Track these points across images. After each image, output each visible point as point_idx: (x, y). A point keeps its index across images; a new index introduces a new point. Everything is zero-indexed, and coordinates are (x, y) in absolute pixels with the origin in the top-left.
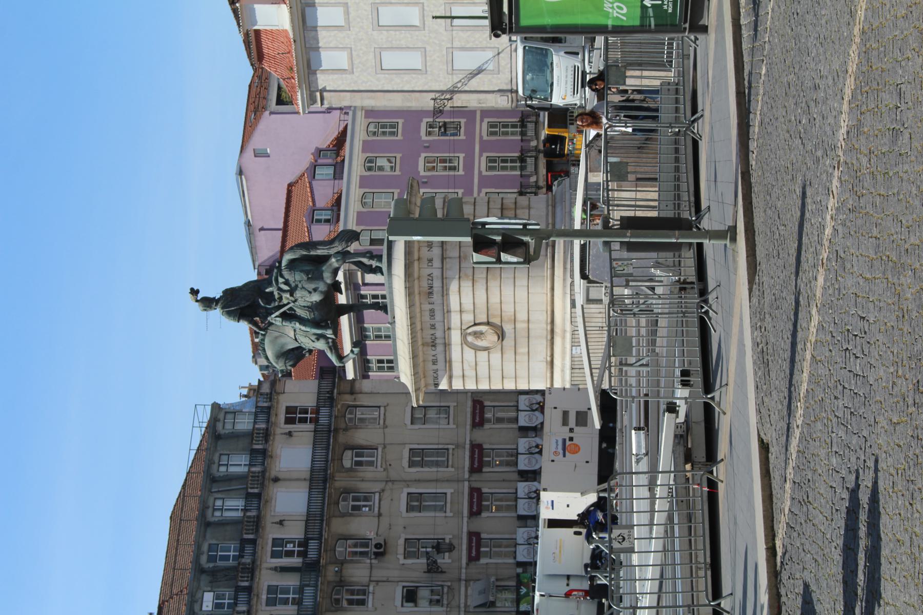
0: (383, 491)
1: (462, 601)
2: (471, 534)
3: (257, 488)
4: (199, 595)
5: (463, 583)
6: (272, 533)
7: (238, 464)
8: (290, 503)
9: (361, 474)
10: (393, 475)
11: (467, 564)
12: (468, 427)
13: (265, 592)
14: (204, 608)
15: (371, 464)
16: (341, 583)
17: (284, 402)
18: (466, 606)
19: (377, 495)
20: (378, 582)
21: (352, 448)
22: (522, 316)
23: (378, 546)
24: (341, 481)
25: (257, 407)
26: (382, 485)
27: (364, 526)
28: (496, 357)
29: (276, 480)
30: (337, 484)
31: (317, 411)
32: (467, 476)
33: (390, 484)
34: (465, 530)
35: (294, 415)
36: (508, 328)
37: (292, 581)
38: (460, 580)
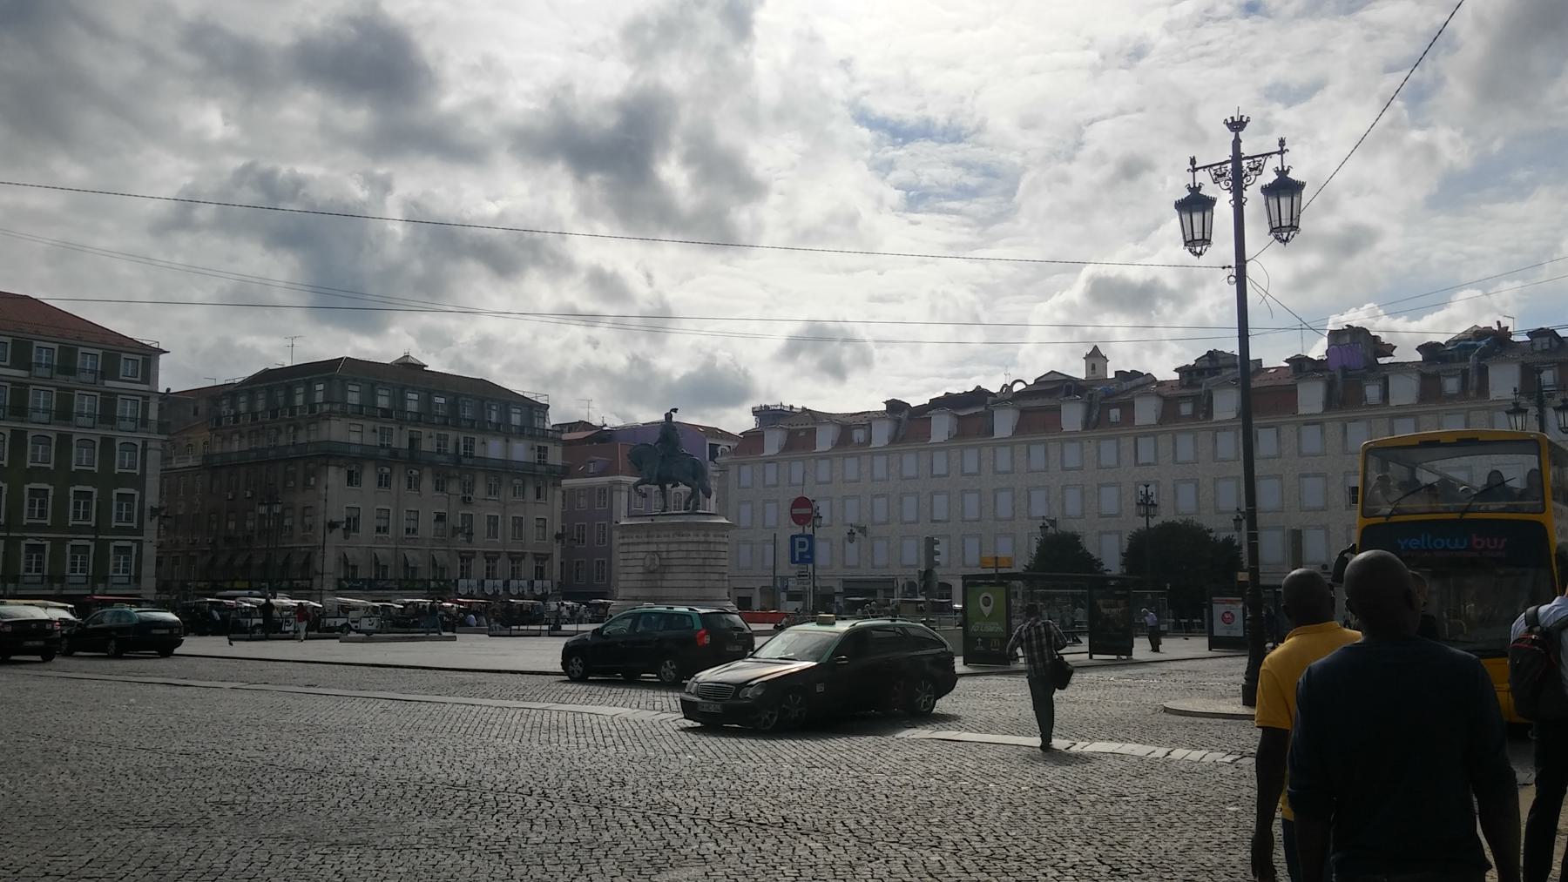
3: (504, 431)
6: (478, 439)
7: (516, 419)
8: (494, 449)
22: (665, 584)
27: (480, 490)
28: (641, 570)
31: (545, 464)
35: (542, 451)
36: (658, 576)
37: (451, 449)
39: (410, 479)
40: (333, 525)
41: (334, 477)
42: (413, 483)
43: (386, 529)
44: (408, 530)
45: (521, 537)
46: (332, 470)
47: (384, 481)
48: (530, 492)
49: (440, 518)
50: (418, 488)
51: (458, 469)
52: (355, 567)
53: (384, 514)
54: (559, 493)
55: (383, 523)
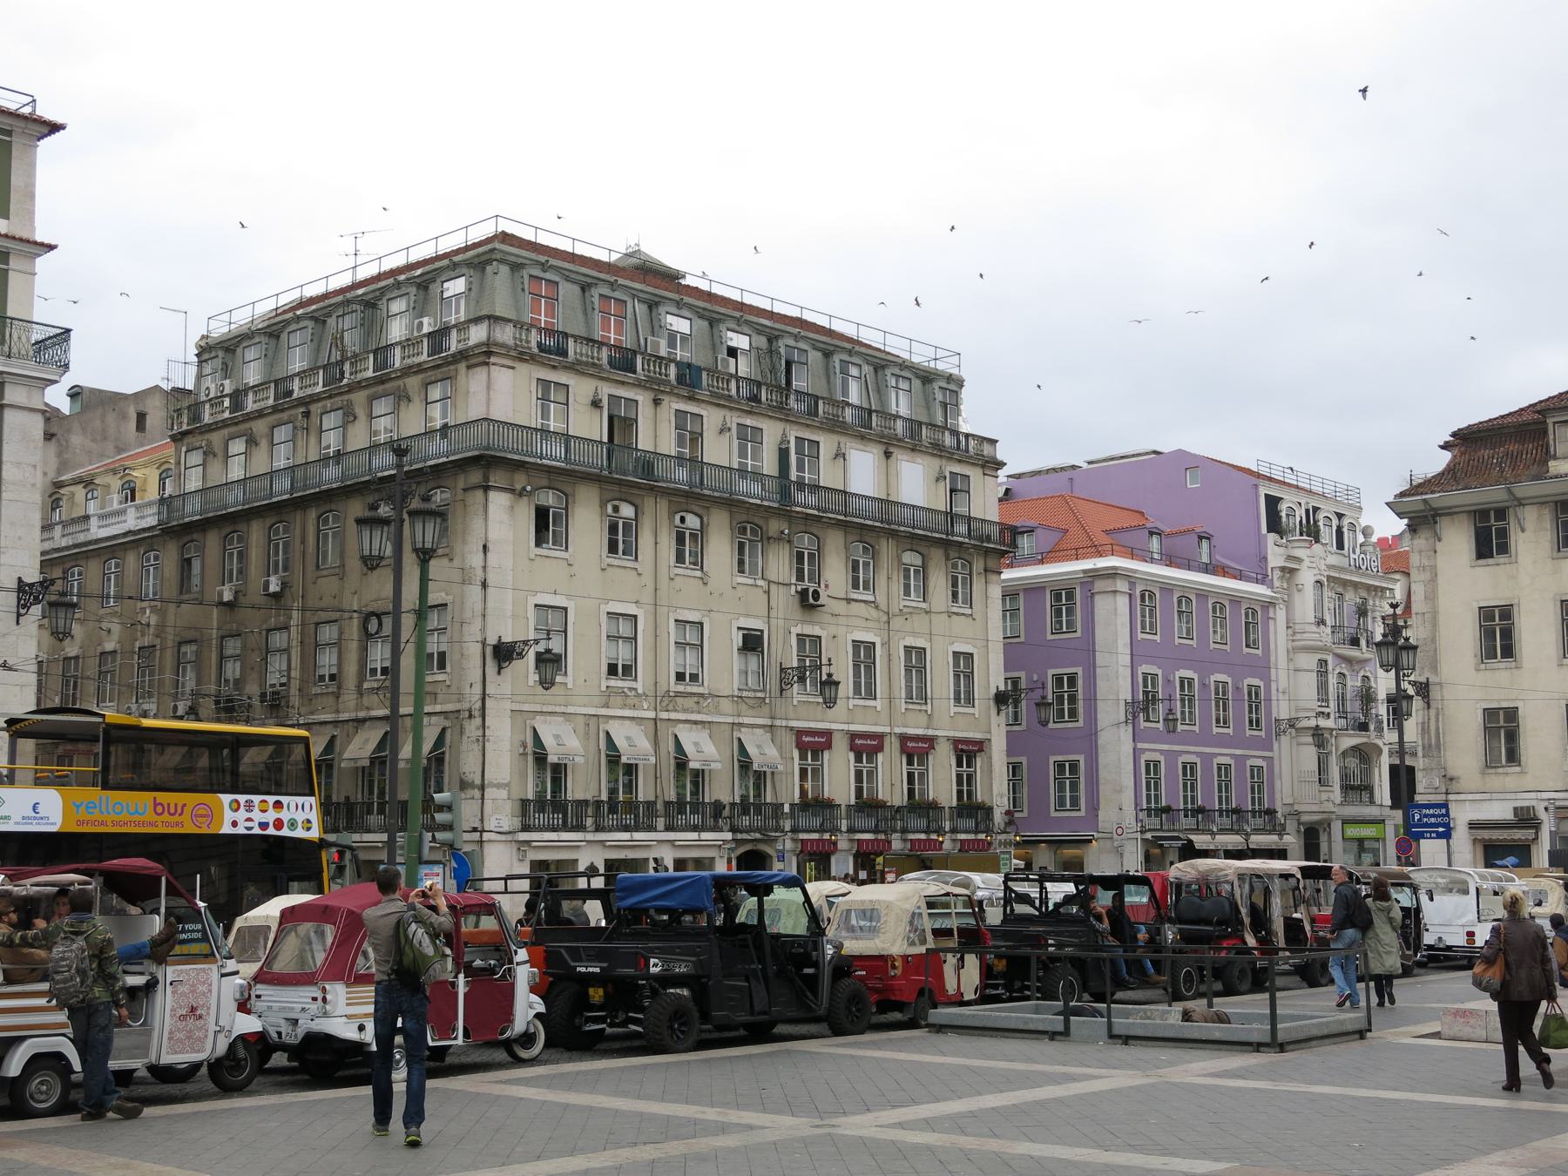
0: (877, 607)
1: (746, 720)
2: (828, 734)
3: (871, 428)
4: (746, 330)
5: (768, 722)
6: (827, 444)
8: (861, 472)
9: (895, 578)
10: (897, 623)
11: (792, 729)
12: (952, 734)
13: (755, 424)
14: (730, 334)
15: (907, 593)
16: (767, 540)
17: (974, 474)
18: (740, 725)
19: (871, 598)
20: (768, 592)
21: (924, 566)
23: (816, 595)
24: (886, 548)
25: (967, 436)
26: (883, 606)
27: (835, 575)
29: (888, 455)
30: (883, 542)
32: (898, 730)
33: (885, 618)
34: (834, 726)
38: (773, 718)
39: (680, 539)
40: (504, 653)
41: (501, 520)
42: (689, 548)
43: (629, 670)
44: (680, 677)
45: (924, 698)
46: (499, 502)
47: (619, 540)
48: (939, 583)
49: (752, 643)
50: (698, 562)
51: (782, 518)
52: (559, 772)
53: (624, 628)
54: (996, 592)
55: (623, 654)
